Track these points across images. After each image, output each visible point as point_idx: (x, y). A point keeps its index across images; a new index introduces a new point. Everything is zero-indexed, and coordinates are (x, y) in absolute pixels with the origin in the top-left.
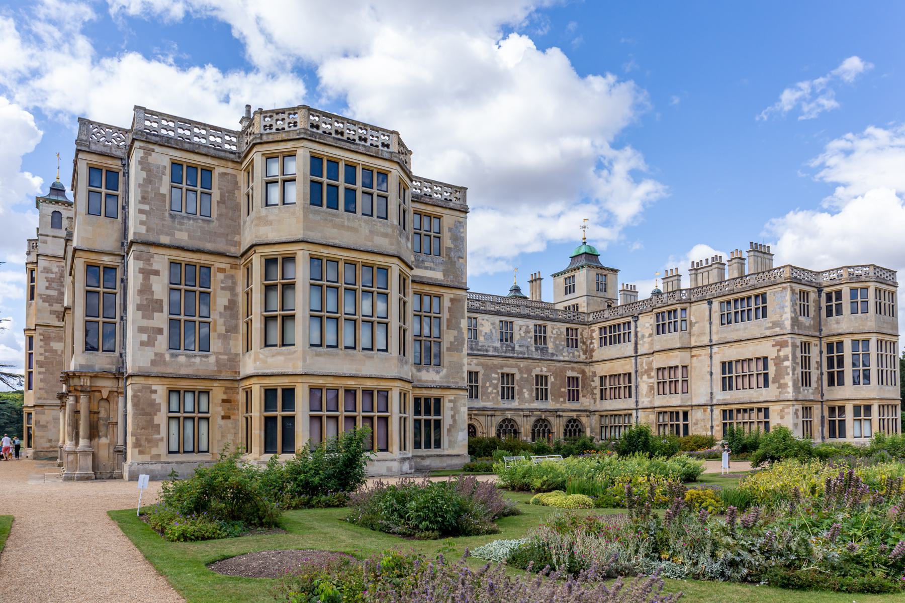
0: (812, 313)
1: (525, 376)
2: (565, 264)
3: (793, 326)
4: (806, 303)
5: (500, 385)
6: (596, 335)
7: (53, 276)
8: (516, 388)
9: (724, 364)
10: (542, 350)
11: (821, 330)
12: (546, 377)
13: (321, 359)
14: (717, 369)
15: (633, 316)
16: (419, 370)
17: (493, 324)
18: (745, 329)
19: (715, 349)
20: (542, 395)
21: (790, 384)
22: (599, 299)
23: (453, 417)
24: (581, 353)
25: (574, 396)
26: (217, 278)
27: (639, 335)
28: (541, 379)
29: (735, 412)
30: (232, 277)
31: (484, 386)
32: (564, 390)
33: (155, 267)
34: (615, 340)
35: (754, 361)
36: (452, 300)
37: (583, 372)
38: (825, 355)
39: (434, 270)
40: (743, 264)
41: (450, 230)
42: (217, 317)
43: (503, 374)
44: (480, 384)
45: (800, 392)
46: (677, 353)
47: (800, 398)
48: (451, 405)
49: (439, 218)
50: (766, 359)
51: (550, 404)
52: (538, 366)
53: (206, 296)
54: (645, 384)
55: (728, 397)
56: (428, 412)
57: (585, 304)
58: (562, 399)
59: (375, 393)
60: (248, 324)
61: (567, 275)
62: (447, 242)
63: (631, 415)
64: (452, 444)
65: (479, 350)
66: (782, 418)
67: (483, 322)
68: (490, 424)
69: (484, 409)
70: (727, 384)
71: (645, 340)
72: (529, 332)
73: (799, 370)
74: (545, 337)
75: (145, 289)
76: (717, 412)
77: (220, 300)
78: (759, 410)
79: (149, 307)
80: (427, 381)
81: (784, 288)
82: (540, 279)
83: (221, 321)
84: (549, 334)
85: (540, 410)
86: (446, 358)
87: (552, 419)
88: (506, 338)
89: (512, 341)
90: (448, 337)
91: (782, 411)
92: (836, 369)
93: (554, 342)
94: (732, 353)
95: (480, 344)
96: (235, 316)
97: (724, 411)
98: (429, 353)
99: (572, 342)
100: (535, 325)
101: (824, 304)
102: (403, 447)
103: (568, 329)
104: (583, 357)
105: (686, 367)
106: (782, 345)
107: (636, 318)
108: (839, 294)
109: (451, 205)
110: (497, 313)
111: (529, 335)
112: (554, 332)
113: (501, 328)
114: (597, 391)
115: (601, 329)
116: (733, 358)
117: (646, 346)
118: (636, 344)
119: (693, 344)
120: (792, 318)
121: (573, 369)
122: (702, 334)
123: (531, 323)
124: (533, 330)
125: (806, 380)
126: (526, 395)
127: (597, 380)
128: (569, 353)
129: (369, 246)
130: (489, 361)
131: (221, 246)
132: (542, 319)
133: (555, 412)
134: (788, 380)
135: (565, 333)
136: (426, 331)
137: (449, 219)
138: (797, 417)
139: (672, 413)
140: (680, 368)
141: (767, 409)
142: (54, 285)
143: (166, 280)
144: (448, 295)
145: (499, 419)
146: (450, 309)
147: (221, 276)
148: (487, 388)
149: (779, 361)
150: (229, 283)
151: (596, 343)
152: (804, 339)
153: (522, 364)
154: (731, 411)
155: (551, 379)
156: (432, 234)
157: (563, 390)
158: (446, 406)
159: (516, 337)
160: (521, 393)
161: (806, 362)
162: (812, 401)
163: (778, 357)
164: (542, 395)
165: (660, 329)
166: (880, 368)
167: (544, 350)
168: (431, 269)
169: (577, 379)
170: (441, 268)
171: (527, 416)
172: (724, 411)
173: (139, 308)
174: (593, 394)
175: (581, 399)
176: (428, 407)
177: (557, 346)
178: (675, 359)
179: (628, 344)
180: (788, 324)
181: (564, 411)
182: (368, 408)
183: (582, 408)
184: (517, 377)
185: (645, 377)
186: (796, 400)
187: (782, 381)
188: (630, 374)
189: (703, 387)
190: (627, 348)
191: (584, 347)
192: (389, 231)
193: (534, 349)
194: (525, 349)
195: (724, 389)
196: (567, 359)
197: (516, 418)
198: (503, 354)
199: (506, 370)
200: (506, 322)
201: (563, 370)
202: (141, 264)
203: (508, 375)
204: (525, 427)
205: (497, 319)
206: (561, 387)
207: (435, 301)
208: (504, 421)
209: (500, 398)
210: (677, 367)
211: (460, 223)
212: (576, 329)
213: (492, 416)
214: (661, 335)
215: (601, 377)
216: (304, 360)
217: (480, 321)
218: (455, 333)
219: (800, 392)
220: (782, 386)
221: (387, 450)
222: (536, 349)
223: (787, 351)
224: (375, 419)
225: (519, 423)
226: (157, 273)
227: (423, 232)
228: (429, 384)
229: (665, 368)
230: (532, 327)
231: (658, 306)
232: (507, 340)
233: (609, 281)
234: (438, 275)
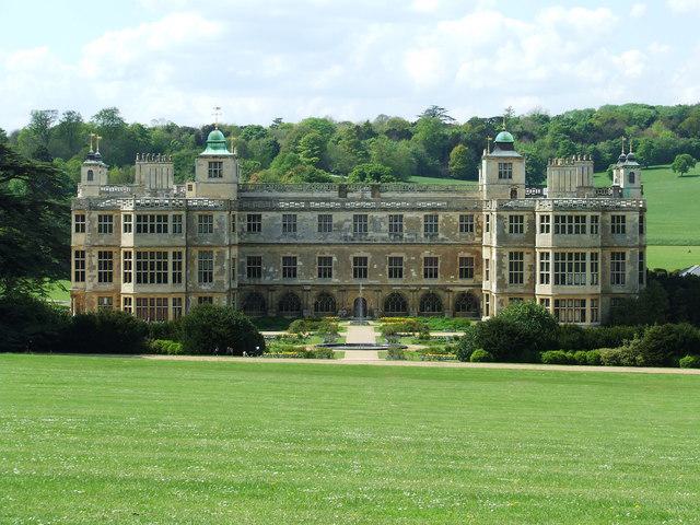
0: (525, 230)
10: (431, 237)
25: (466, 273)
28: (430, 261)
37: (479, 254)
86: (214, 280)
87: (441, 293)
90: (216, 269)
100: (426, 216)
103: (461, 216)
104: (477, 239)
110: (386, 209)
121: (465, 251)
123: (421, 215)
124: (422, 221)
130: (377, 249)
133: (444, 288)
145: (386, 293)
160: (408, 272)
166: (560, 272)
199: (393, 255)
200: (396, 216)
203: (396, 258)
208: (393, 295)
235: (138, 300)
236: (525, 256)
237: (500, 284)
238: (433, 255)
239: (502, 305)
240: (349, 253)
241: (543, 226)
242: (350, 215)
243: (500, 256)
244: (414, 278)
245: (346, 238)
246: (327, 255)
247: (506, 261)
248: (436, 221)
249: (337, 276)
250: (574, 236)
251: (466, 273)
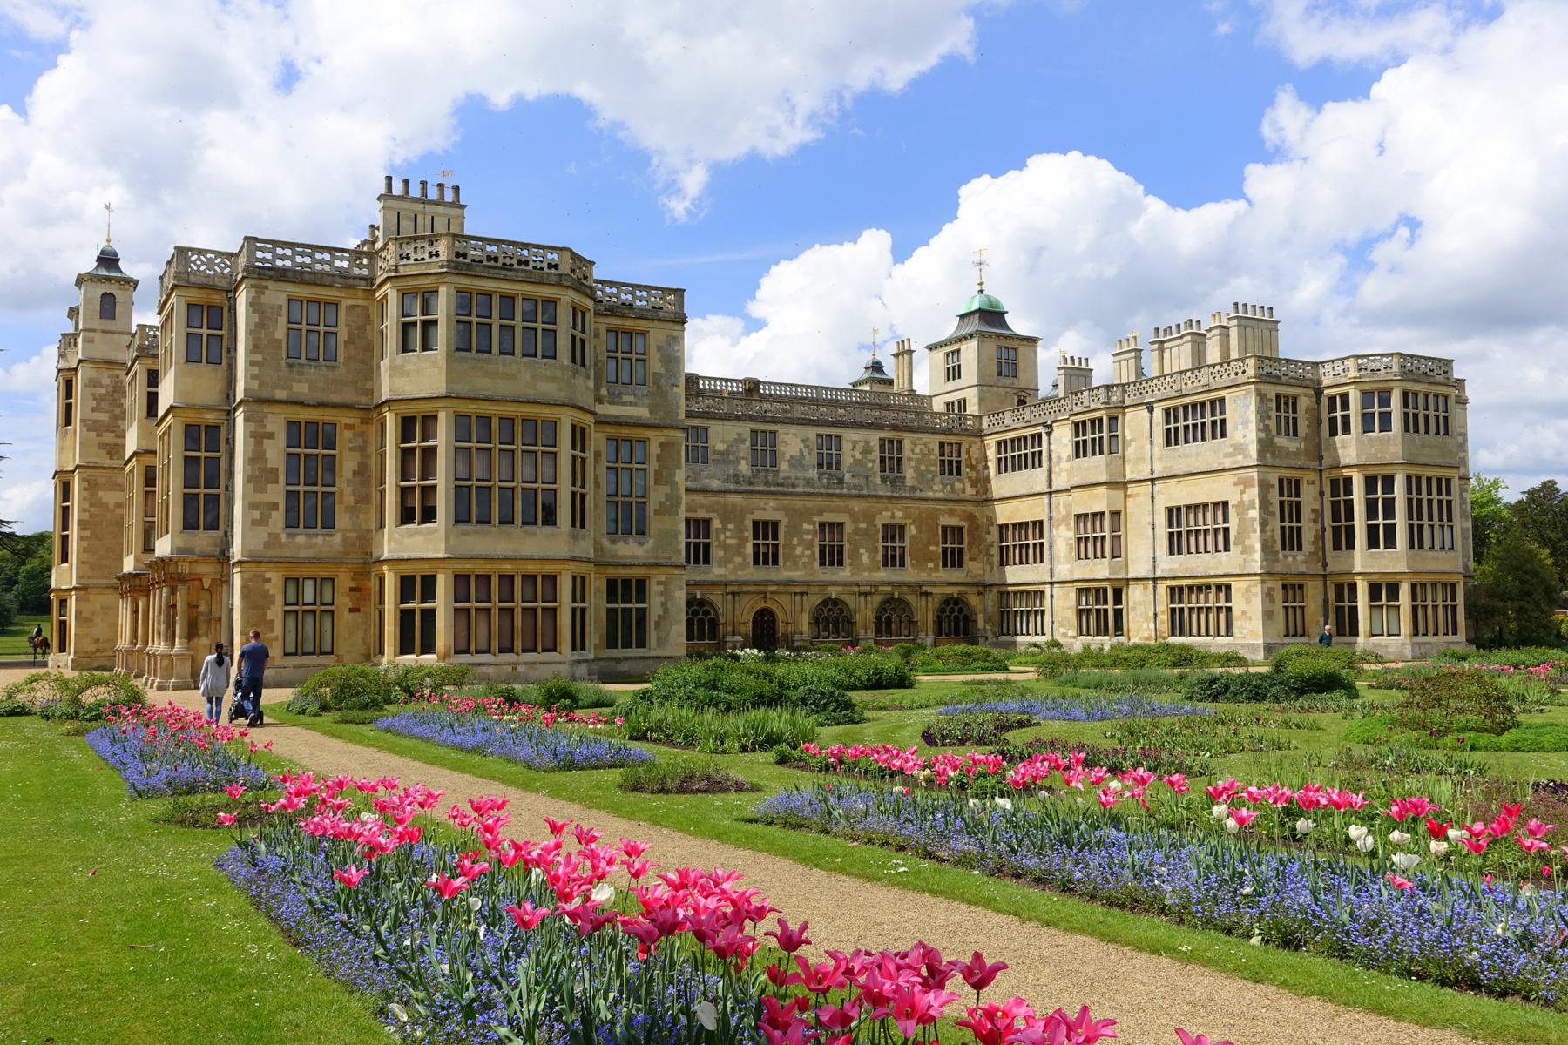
1: (863, 526)
2: (950, 329)
3: (1261, 453)
4: (1291, 415)
5: (817, 542)
6: (992, 453)
7: (103, 391)
8: (847, 546)
9: (1170, 510)
10: (894, 482)
11: (1321, 458)
12: (902, 527)
13: (469, 539)
14: (1161, 519)
15: (1044, 425)
16: (614, 542)
17: (804, 440)
18: (1198, 454)
19: (1159, 485)
20: (893, 559)
21: (1258, 546)
22: (1002, 391)
23: (664, 604)
24: (968, 485)
25: (953, 558)
26: (344, 438)
27: (1054, 456)
28: (894, 532)
29: (1186, 591)
30: (362, 434)
31: (789, 545)
32: (936, 549)
33: (269, 428)
34: (1021, 463)
35: (1211, 507)
36: (662, 445)
37: (971, 518)
38: (1328, 498)
39: (636, 405)
40: (1228, 336)
41: (659, 348)
42: (344, 485)
43: (822, 525)
44: (781, 540)
45: (1277, 561)
46: (1103, 490)
47: (1278, 569)
48: (661, 588)
49: (644, 334)
50: (1225, 504)
51: (910, 574)
52: (887, 509)
53: (331, 465)
54: (1062, 538)
55: (1177, 566)
56: (627, 600)
57: (976, 400)
58: (931, 565)
59: (539, 579)
60: (382, 493)
61: (949, 349)
62: (655, 366)
63: (1043, 592)
64: (661, 642)
65: (778, 485)
66: (1248, 602)
67: (787, 438)
68: (798, 608)
69: (789, 583)
70: (1175, 544)
71: (1065, 465)
72: (870, 452)
73: (1275, 524)
74: (900, 460)
75: (256, 458)
76: (1162, 588)
77: (348, 464)
78: (1219, 587)
79: (260, 475)
80: (626, 557)
81: (1248, 392)
82: (911, 352)
83: (348, 490)
84: (906, 452)
85: (889, 584)
86: (654, 524)
88: (829, 462)
89: (839, 465)
90: (656, 496)
91: (1248, 590)
92: (1343, 523)
93: (916, 469)
94: (1182, 493)
95: (782, 475)
96: (366, 483)
97: (1172, 589)
98: (629, 517)
99: (951, 468)
101: (1325, 416)
102: (579, 643)
103: (942, 445)
105: (1119, 513)
106: (1245, 483)
107: (1050, 429)
108: (1345, 398)
109: (661, 314)
110: (811, 423)
111: (869, 457)
112: (917, 450)
113: (820, 448)
114: (995, 551)
115: (999, 443)
116: (1181, 503)
117: (1064, 474)
118: (1050, 471)
119: (1129, 477)
120: (1260, 441)
121: (951, 513)
122: (1140, 460)
123: (874, 438)
124: (877, 448)
125: (1291, 539)
126: (865, 558)
127: (994, 531)
128: (945, 486)
129: (531, 394)
130: (798, 503)
131: (348, 396)
132: (894, 428)
134: (1255, 541)
135: (937, 451)
136: (624, 489)
137: (657, 334)
138: (1272, 601)
139: (1097, 590)
140: (1107, 515)
141: (1228, 587)
142: (105, 405)
143: (283, 444)
144: (655, 439)
145: (816, 599)
146: (659, 457)
147: (348, 434)
148: (794, 548)
149: (1243, 508)
150: (359, 441)
151: (992, 466)
152: (1285, 474)
153: (857, 506)
154: (1181, 588)
155: (912, 531)
156: (634, 356)
157: (932, 548)
158: (654, 589)
159: (847, 461)
160: (855, 555)
161: (1291, 511)
162: (1302, 574)
163: (1241, 503)
164: (893, 559)
165: (1080, 450)
167: (898, 482)
168: (631, 404)
169: (960, 529)
170: (647, 401)
171: (866, 594)
172: (1172, 589)
173: (249, 479)
174: (990, 555)
175: (969, 564)
176: (627, 587)
177: (920, 475)
178: (1099, 501)
179: (1038, 470)
180: (1253, 449)
181: (934, 584)
182: (529, 595)
183: (969, 580)
184: (848, 529)
185: (1063, 528)
186: (1269, 574)
187: (1247, 542)
188: (1041, 522)
189: (1145, 550)
190: (1034, 479)
191: (973, 475)
192: (558, 373)
193: (878, 480)
194: (862, 481)
195: (1171, 553)
196: (940, 495)
197: (846, 598)
198: (822, 490)
199: (828, 517)
200: (829, 436)
201: (934, 515)
202: (252, 426)
203: (831, 525)
204: (865, 612)
205: (812, 433)
206: (930, 543)
207: (638, 449)
208: (825, 602)
209: (817, 564)
210: (1103, 513)
211: (674, 338)
212: (959, 444)
213: (802, 594)
214: (1082, 459)
215: (1001, 527)
216: (447, 540)
217: (781, 437)
218: (667, 489)
219: (1277, 561)
220: (1247, 550)
221: (555, 650)
222: (884, 480)
223: (1253, 493)
224: (539, 612)
225: (852, 606)
226: (271, 436)
227: (620, 355)
228: (628, 561)
229: (1086, 515)
230: (875, 443)
231: (1077, 409)
232: (829, 466)
233: (1021, 358)
234: (642, 412)
235: (461, 580)
236: (1304, 488)
237: (1266, 548)
238: (897, 521)
239: (1272, 601)
240: (743, 512)
241: (1333, 421)
242: (746, 428)
243: (1264, 486)
244: (863, 568)
245: (736, 478)
246: (701, 514)
247: (1275, 498)
248: (900, 451)
249: (723, 562)
250: (1431, 437)
251: (953, 558)
